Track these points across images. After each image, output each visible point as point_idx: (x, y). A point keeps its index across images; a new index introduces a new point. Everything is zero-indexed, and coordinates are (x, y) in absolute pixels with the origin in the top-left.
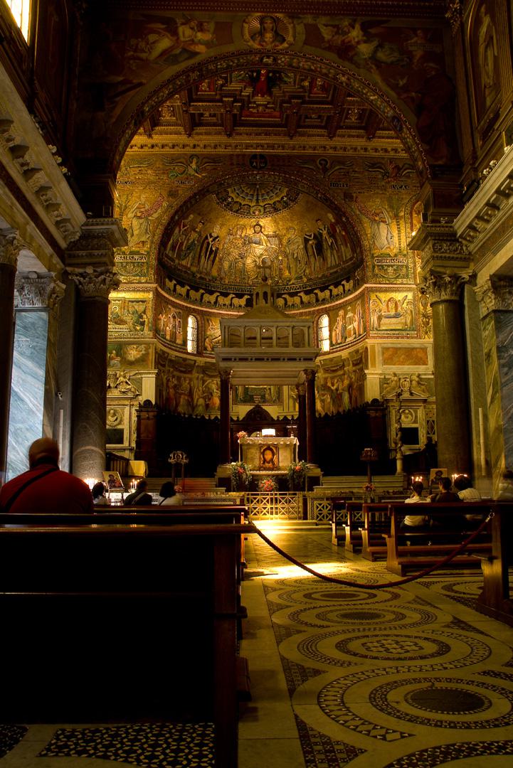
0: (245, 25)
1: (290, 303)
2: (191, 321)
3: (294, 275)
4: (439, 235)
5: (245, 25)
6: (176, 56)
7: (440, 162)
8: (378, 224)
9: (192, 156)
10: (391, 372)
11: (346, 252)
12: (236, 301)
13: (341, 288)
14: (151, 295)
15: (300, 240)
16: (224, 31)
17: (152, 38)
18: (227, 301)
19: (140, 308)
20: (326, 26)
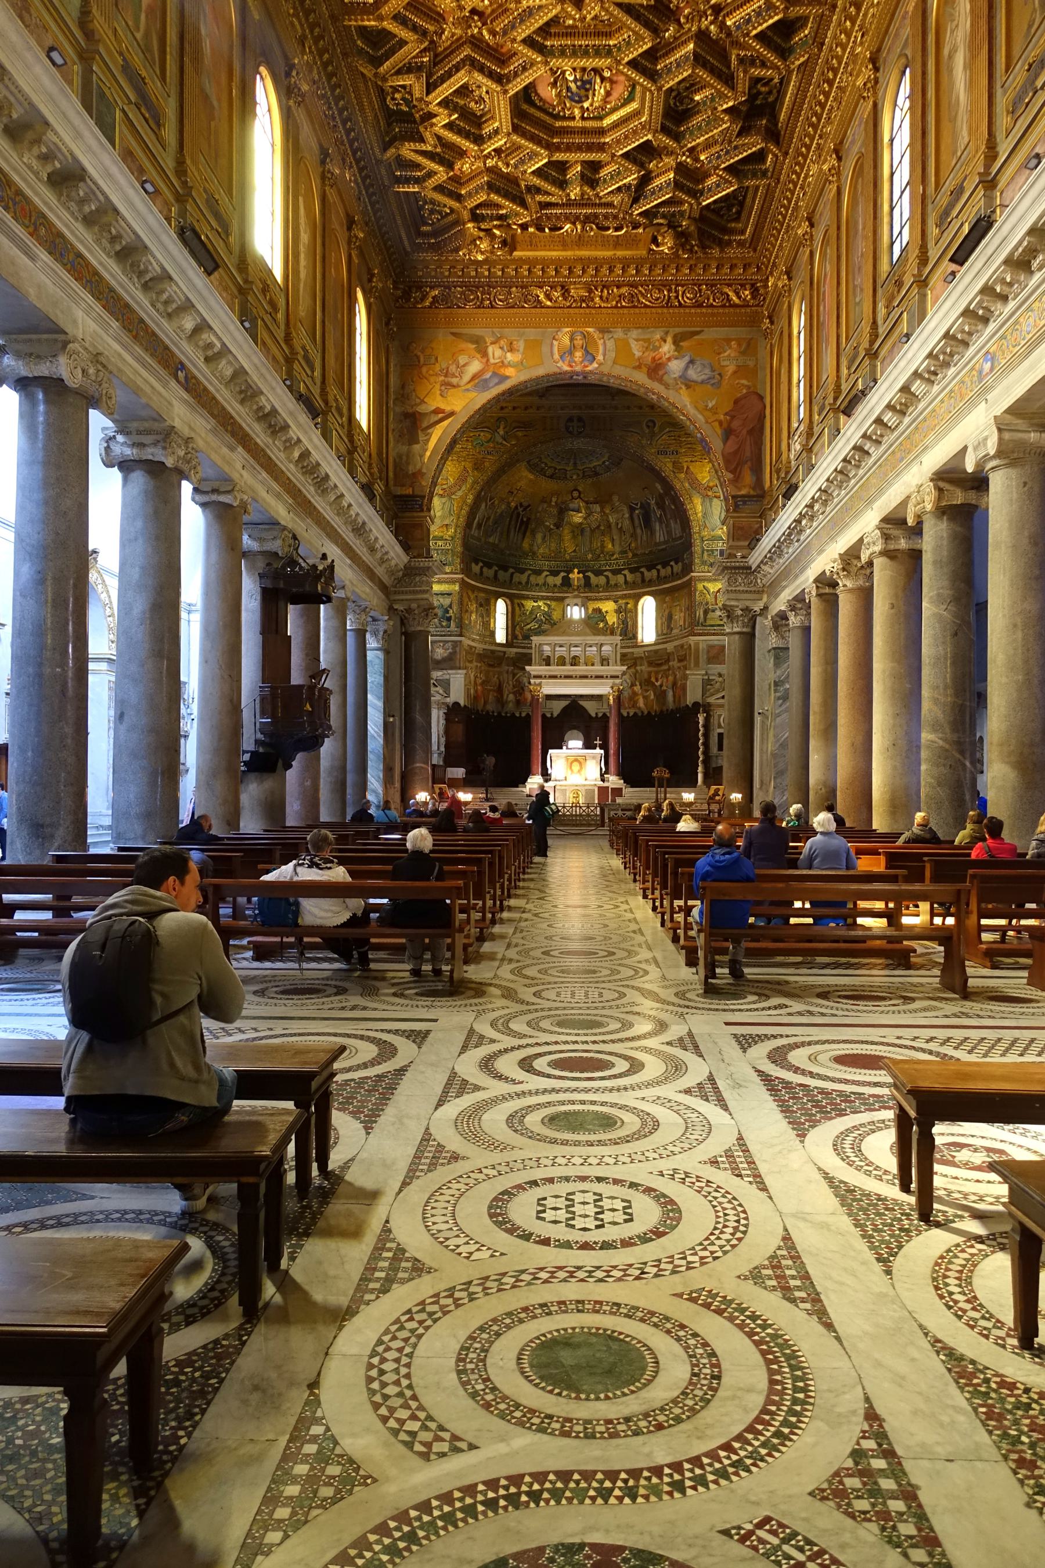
0: (555, 343)
1: (612, 582)
2: (501, 606)
3: (617, 549)
4: (735, 568)
5: (555, 343)
6: (486, 380)
7: (743, 492)
8: (711, 502)
9: (499, 419)
10: (716, 672)
11: (676, 528)
12: (551, 580)
13: (669, 569)
14: (457, 587)
15: (625, 509)
16: (533, 346)
17: (462, 359)
18: (540, 580)
19: (446, 601)
20: (637, 340)
